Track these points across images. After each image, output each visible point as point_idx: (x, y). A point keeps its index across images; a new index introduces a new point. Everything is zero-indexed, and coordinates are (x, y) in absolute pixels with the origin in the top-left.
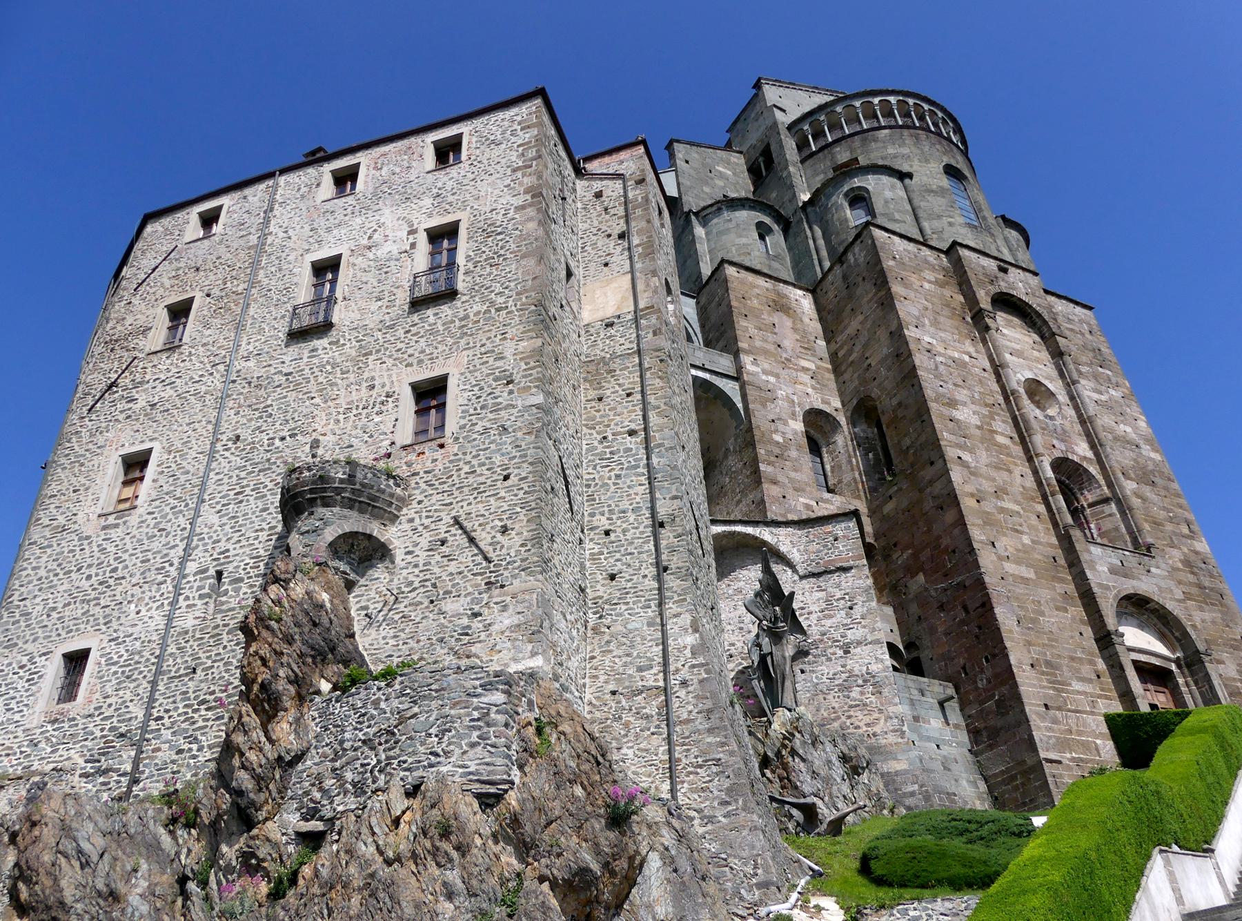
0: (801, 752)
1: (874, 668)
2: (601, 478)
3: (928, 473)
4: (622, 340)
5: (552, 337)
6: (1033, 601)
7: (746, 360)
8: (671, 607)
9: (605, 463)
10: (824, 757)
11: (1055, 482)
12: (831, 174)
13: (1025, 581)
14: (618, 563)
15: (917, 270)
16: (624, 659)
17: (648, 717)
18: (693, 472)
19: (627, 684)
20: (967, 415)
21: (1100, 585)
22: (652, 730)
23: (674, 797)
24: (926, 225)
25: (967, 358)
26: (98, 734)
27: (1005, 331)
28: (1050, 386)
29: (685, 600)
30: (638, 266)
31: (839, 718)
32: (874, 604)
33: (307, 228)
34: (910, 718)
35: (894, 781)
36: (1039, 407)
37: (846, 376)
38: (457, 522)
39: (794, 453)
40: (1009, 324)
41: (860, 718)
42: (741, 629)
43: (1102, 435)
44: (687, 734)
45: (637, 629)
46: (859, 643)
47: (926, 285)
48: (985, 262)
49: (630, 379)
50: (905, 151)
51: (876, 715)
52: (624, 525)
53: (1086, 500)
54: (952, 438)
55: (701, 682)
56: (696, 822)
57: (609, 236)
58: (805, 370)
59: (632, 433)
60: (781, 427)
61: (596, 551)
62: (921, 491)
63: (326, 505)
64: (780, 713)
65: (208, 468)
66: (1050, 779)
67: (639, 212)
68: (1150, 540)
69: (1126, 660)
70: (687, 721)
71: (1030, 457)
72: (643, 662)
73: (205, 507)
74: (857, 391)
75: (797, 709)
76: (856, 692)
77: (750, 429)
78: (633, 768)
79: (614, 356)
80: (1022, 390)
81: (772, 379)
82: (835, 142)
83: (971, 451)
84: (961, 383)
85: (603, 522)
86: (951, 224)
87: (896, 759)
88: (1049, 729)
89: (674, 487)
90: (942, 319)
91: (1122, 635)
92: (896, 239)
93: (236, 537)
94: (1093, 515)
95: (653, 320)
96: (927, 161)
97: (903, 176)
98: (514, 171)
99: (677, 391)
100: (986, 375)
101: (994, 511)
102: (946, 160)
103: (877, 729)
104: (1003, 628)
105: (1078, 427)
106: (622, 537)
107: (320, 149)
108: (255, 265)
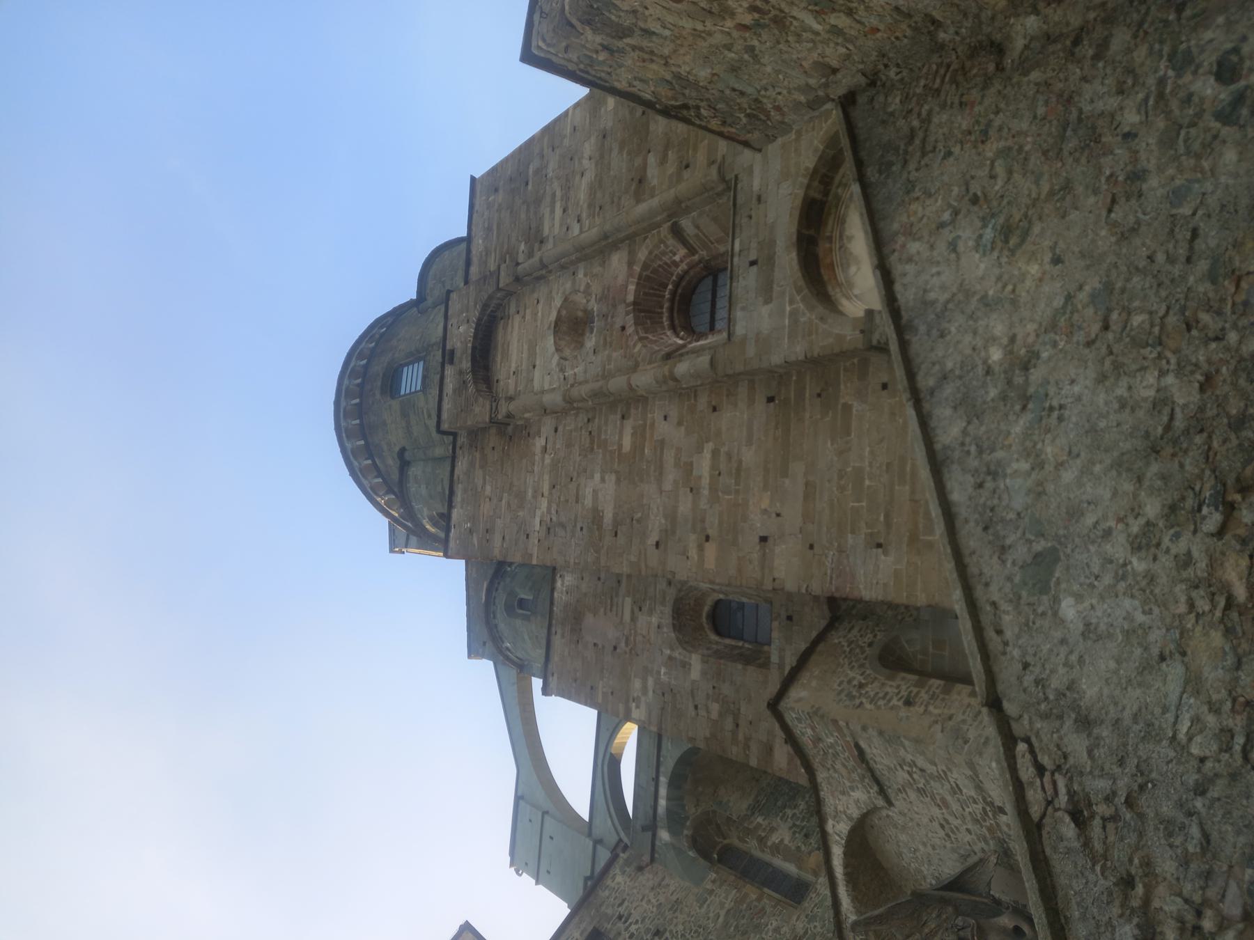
6: (842, 489)
13: (810, 491)
27: (513, 369)
28: (558, 302)
46: (979, 787)
47: (488, 488)
48: (449, 387)
81: (650, 682)
100: (560, 429)
102: (378, 396)
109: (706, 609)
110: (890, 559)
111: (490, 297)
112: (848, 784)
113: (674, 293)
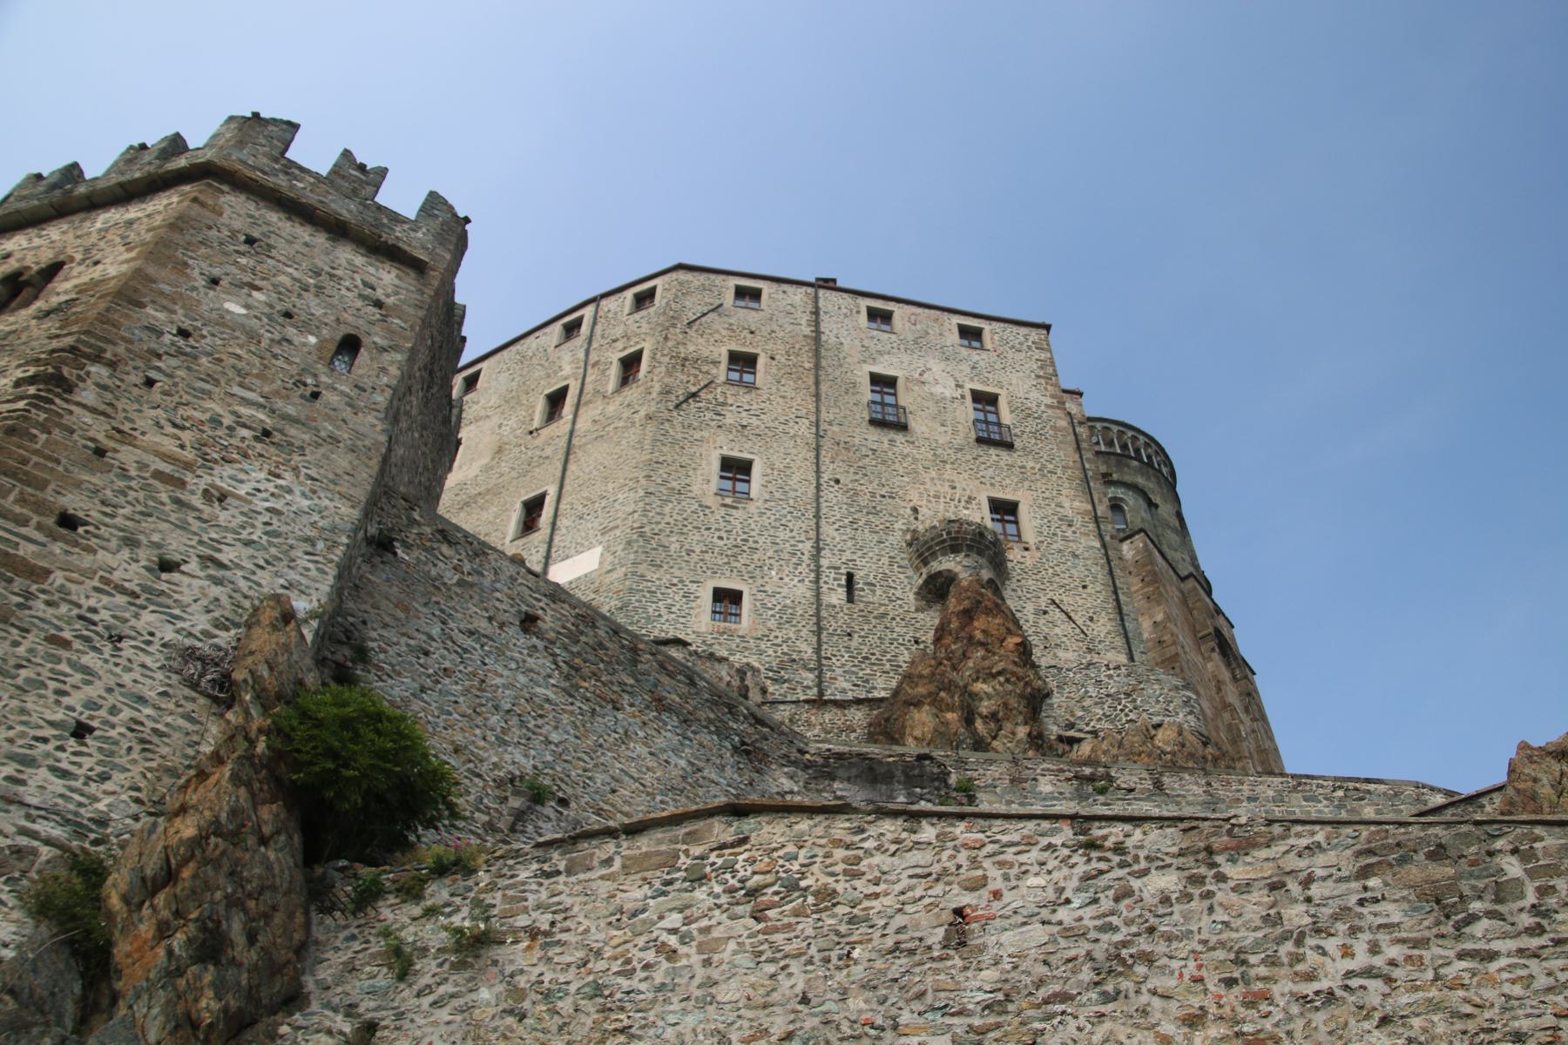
26: (770, 652)
33: (857, 342)
38: (1054, 602)
63: (980, 553)
65: (818, 498)
73: (823, 522)
93: (860, 553)
97: (1152, 505)
98: (1038, 377)
107: (834, 281)
108: (817, 355)
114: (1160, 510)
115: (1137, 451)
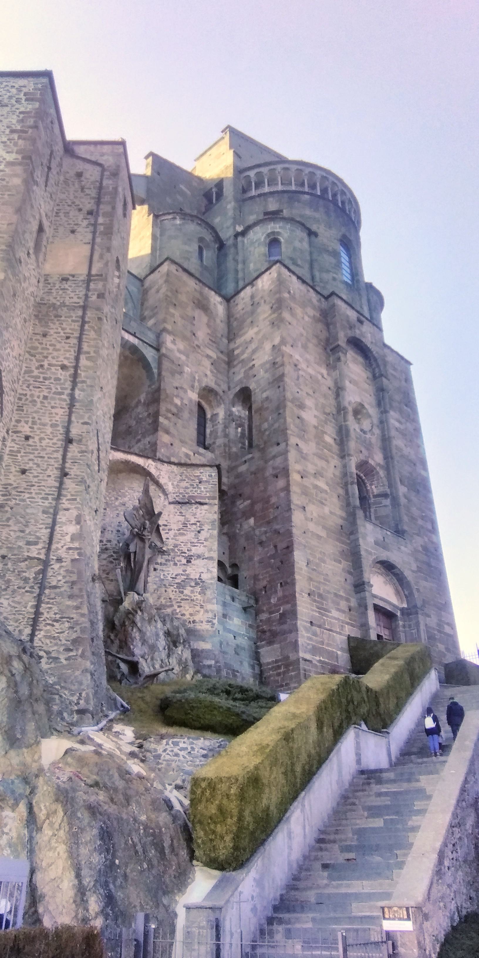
0: (139, 625)
1: (204, 577)
2: (32, 396)
3: (275, 450)
4: (72, 295)
5: (15, 275)
6: (321, 552)
7: (168, 339)
8: (65, 503)
9: (37, 384)
10: (155, 631)
11: (355, 476)
12: (261, 217)
13: (319, 537)
14: (31, 462)
15: (303, 305)
16: (19, 534)
17: (26, 580)
18: (106, 409)
19: (16, 552)
20: (310, 416)
21: (366, 551)
22: (27, 589)
23: (32, 641)
24: (317, 274)
25: (320, 377)
29: (75, 499)
30: (98, 240)
31: (172, 606)
32: (215, 532)
34: (221, 614)
35: (199, 656)
36: (359, 423)
37: (236, 369)
39: (186, 415)
40: (355, 361)
41: (187, 610)
42: (118, 531)
43: (394, 451)
44: (53, 596)
45: (33, 514)
46: (199, 557)
47: (307, 318)
49: (71, 326)
50: (317, 215)
51: (198, 608)
52: (42, 435)
53: (373, 493)
54: (296, 430)
55: (73, 560)
56: (43, 661)
57: (80, 210)
58: (208, 356)
59: (64, 367)
60: (181, 393)
61: (15, 449)
62: (266, 462)
64: (131, 596)
66: (302, 672)
67: (107, 198)
68: (406, 528)
69: (370, 603)
70: (55, 587)
71: (343, 455)
72: (32, 539)
74: (241, 381)
75: (144, 595)
76: (187, 591)
77: (158, 390)
78: (5, 615)
79: (63, 304)
80: (350, 409)
81: (183, 358)
82: (271, 193)
83: (306, 441)
84: (311, 392)
85: (26, 429)
86: (334, 279)
87: (203, 641)
88: (310, 639)
89: (87, 416)
90: (310, 345)
91: (372, 586)
92: (294, 278)
94: (375, 503)
95: (100, 285)
96: (330, 228)
97: (311, 234)
99: (106, 344)
100: (330, 392)
101: (311, 487)
103: (197, 618)
104: (296, 565)
105: (379, 444)
106: (38, 444)
109: (203, 403)
110: (305, 568)
111: (378, 366)
112: (175, 483)
113: (361, 478)
114: (320, 238)
115: (313, 186)
